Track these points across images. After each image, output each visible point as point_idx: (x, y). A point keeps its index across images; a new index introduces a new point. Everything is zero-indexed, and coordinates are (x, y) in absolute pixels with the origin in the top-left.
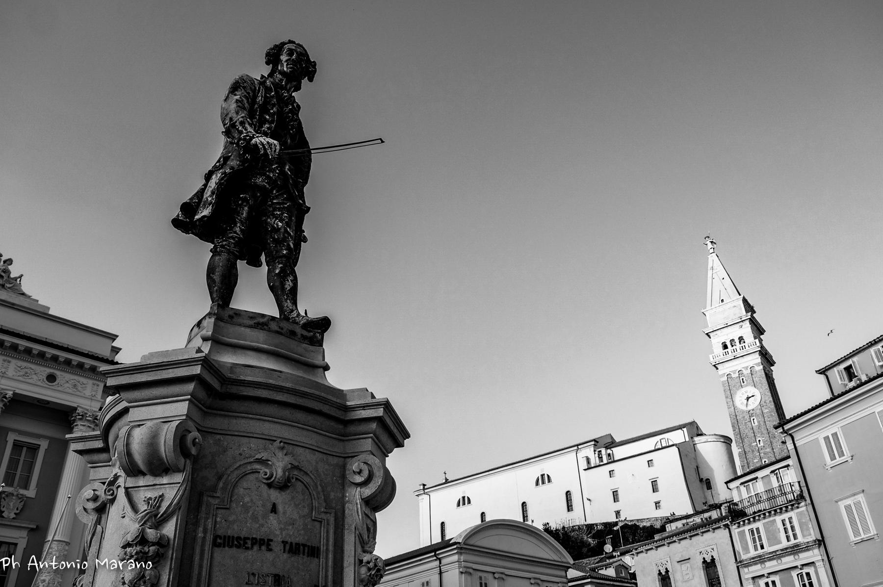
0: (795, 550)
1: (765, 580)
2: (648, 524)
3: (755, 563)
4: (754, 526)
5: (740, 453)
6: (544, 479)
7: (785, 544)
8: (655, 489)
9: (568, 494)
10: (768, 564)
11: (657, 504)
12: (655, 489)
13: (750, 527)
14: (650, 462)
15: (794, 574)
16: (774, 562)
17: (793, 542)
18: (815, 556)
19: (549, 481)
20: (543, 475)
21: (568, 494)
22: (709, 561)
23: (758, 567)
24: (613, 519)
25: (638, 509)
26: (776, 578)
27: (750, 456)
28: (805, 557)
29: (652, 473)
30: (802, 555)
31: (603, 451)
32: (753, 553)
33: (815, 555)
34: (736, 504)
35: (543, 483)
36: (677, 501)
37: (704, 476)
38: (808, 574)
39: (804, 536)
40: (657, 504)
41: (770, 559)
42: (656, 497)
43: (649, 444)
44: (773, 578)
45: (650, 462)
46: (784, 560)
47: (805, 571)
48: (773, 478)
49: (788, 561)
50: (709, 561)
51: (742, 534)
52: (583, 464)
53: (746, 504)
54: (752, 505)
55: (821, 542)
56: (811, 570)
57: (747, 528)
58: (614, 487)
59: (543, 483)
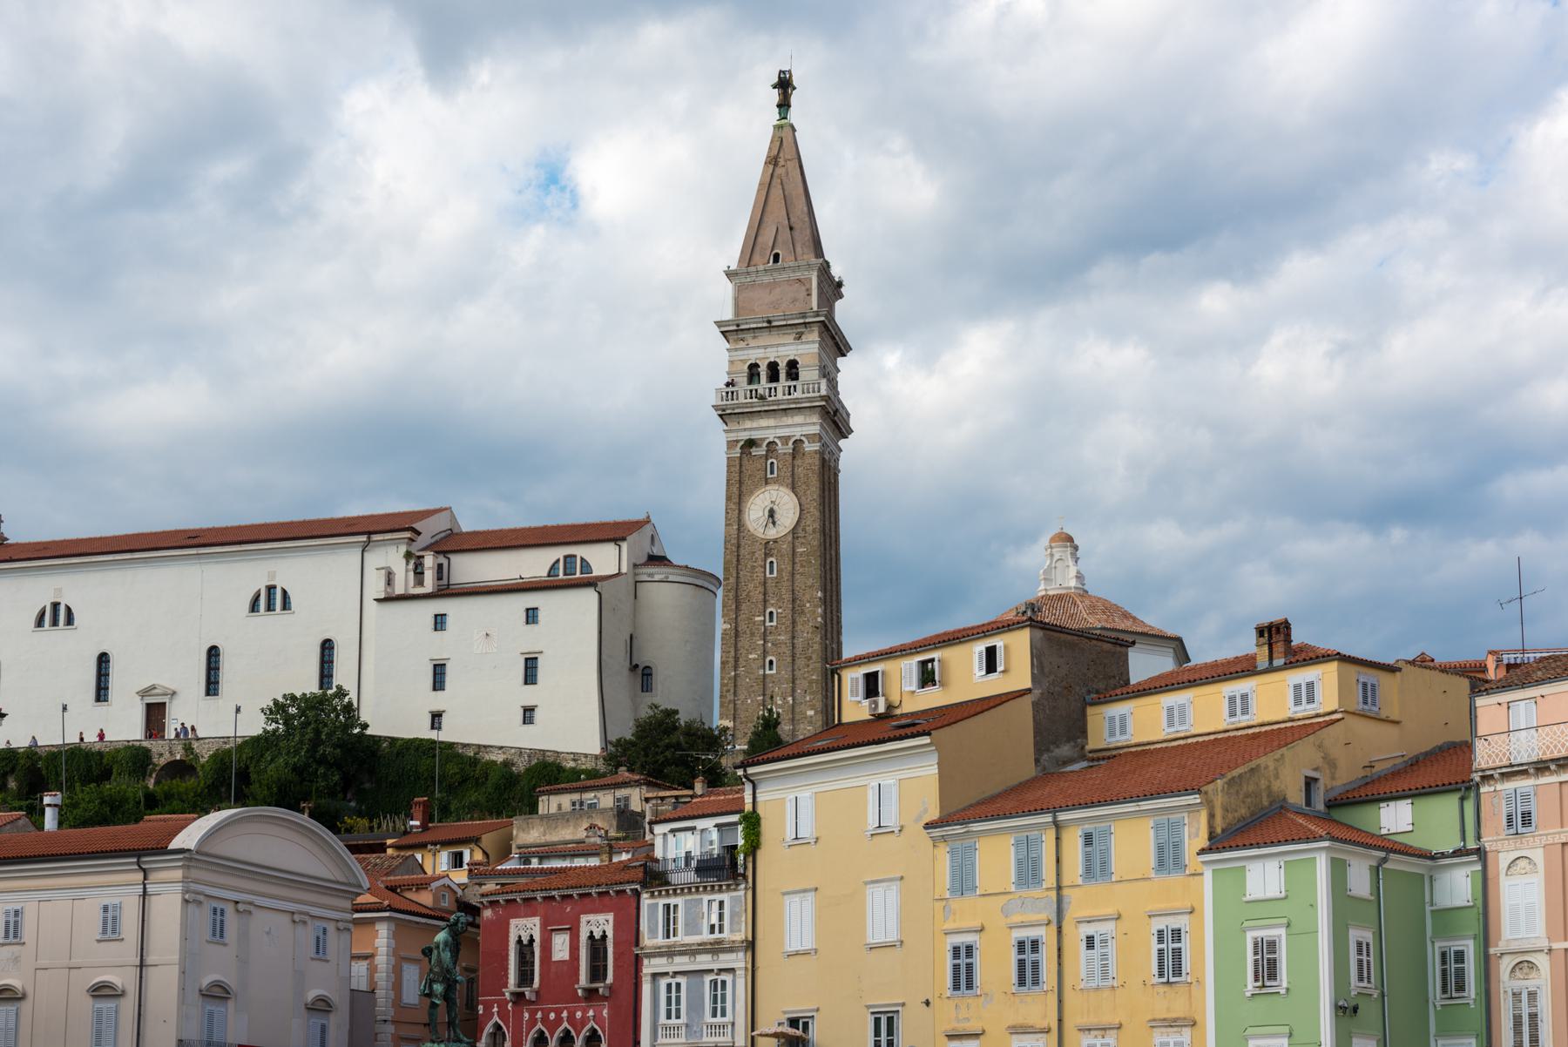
0: (716, 948)
1: (669, 980)
2: (499, 758)
3: (661, 955)
4: (672, 901)
5: (725, 633)
6: (271, 600)
7: (706, 936)
8: (530, 675)
9: (327, 647)
10: (677, 959)
11: (528, 714)
12: (530, 675)
13: (667, 901)
14: (531, 616)
15: (708, 978)
16: (685, 959)
17: (717, 935)
18: (736, 961)
19: (286, 605)
20: (271, 589)
21: (327, 647)
22: (597, 935)
23: (663, 960)
24: (424, 732)
25: (484, 718)
26: (682, 980)
27: (744, 642)
28: (726, 960)
29: (530, 640)
30: (723, 957)
31: (429, 561)
32: (660, 940)
33: (738, 960)
34: (657, 861)
35: (270, 607)
36: (572, 724)
37: (643, 659)
38: (724, 982)
39: (732, 931)
40: (528, 714)
41: (682, 953)
42: (530, 695)
43: (536, 563)
44: (680, 979)
45: (531, 616)
46: (700, 958)
47: (720, 978)
48: (715, 835)
49: (704, 962)
50: (597, 935)
51: (653, 907)
52: (375, 587)
53: (671, 866)
54: (678, 870)
55: (751, 945)
56: (728, 978)
57: (662, 902)
58: (439, 655)
59: (270, 607)
